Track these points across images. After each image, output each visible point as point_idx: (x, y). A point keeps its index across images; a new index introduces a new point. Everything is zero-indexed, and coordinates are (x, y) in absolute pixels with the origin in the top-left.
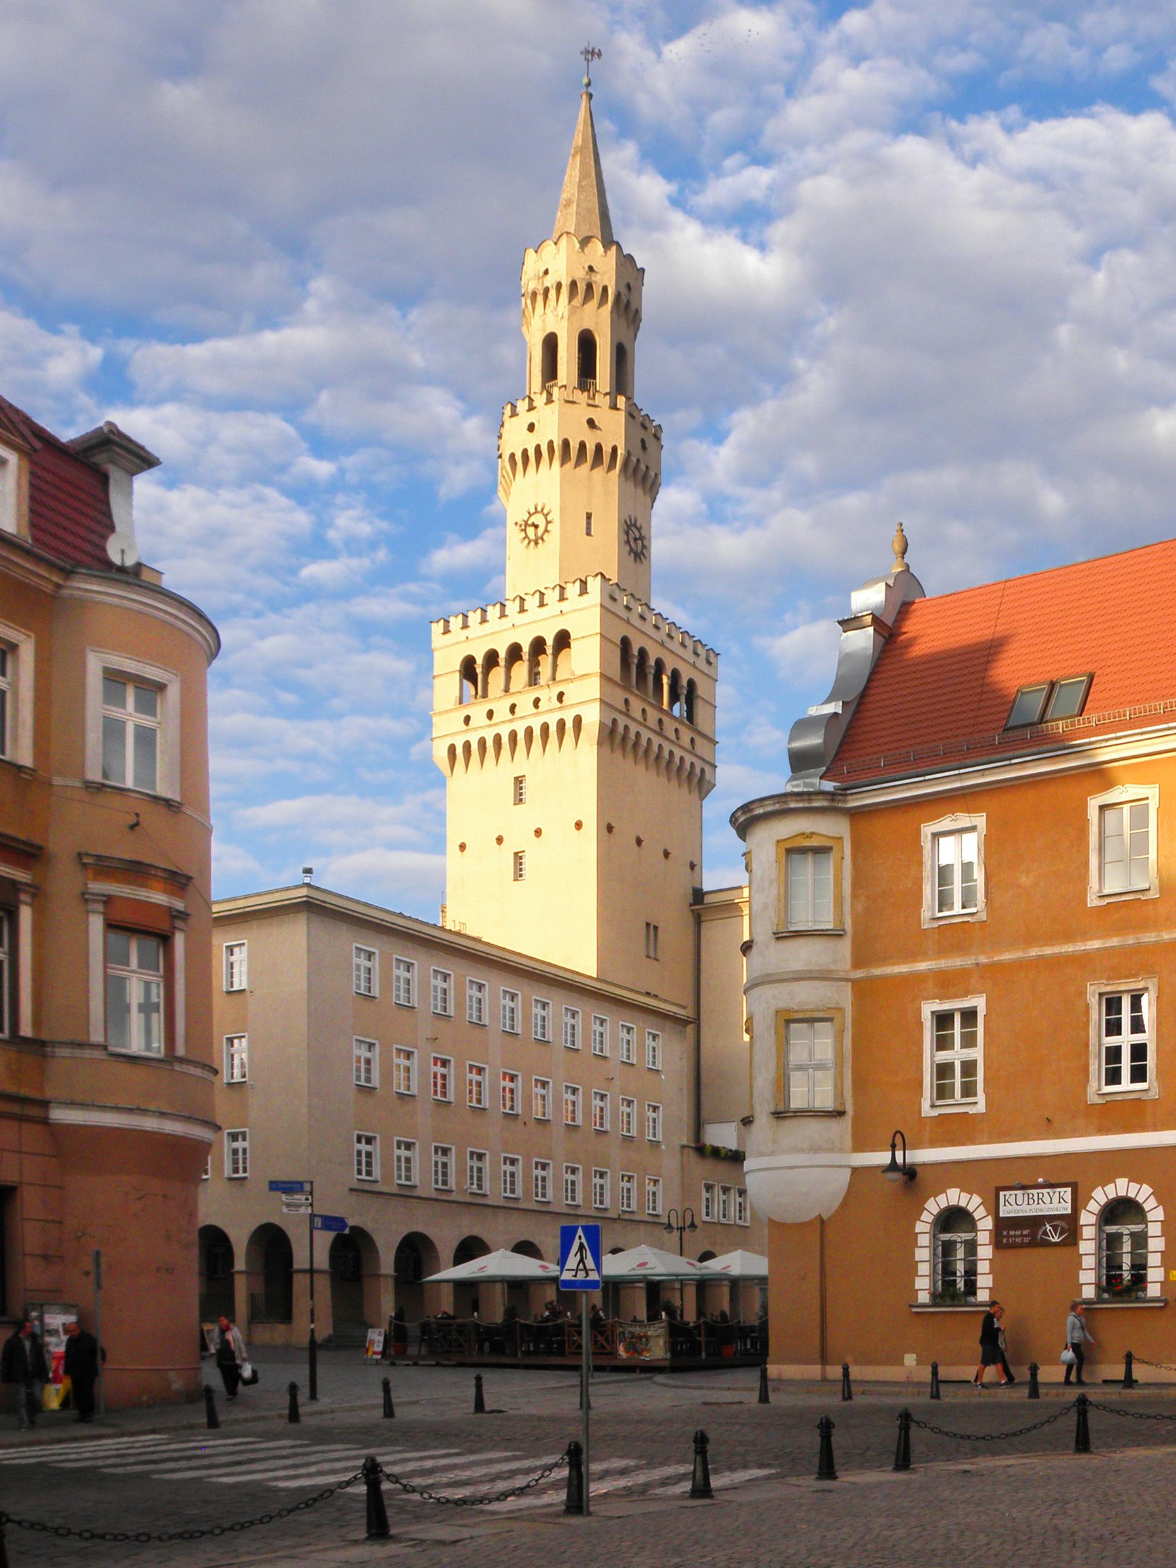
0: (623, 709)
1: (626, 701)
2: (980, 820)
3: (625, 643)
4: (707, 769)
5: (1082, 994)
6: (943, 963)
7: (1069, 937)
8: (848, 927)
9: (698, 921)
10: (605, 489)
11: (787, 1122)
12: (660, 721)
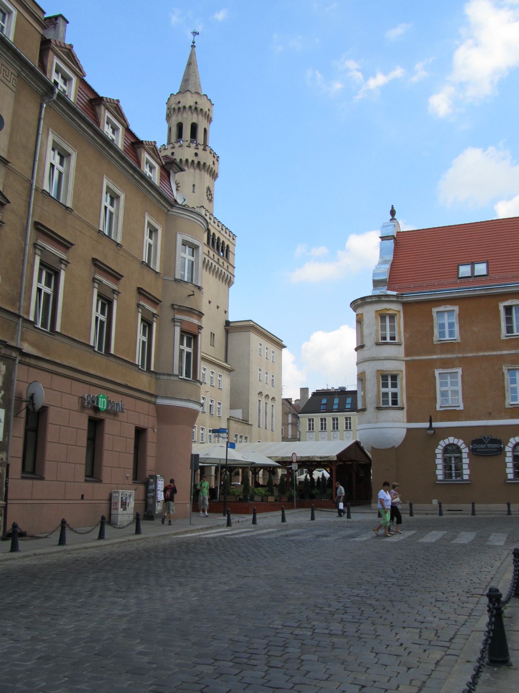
0: (208, 254)
1: (209, 251)
2: (456, 308)
4: (232, 277)
5: (501, 369)
6: (443, 356)
7: (494, 349)
8: (403, 341)
11: (383, 411)
12: (218, 259)
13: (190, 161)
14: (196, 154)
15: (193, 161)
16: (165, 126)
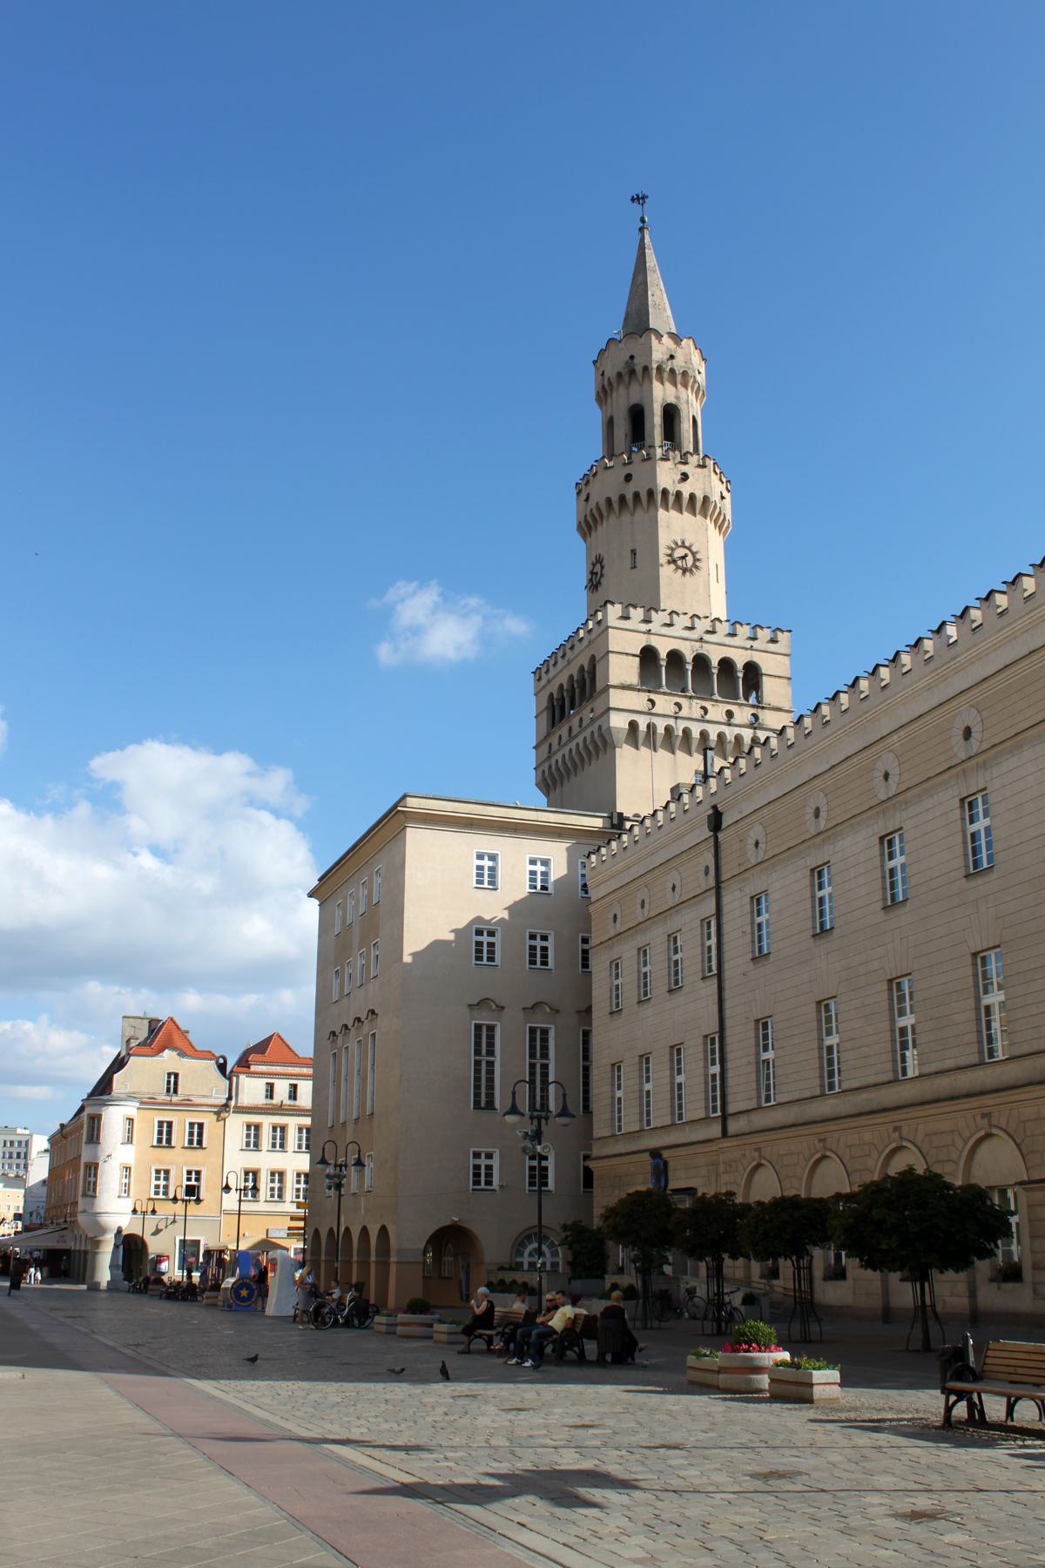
14: (685, 477)
15: (679, 495)
16: (593, 418)
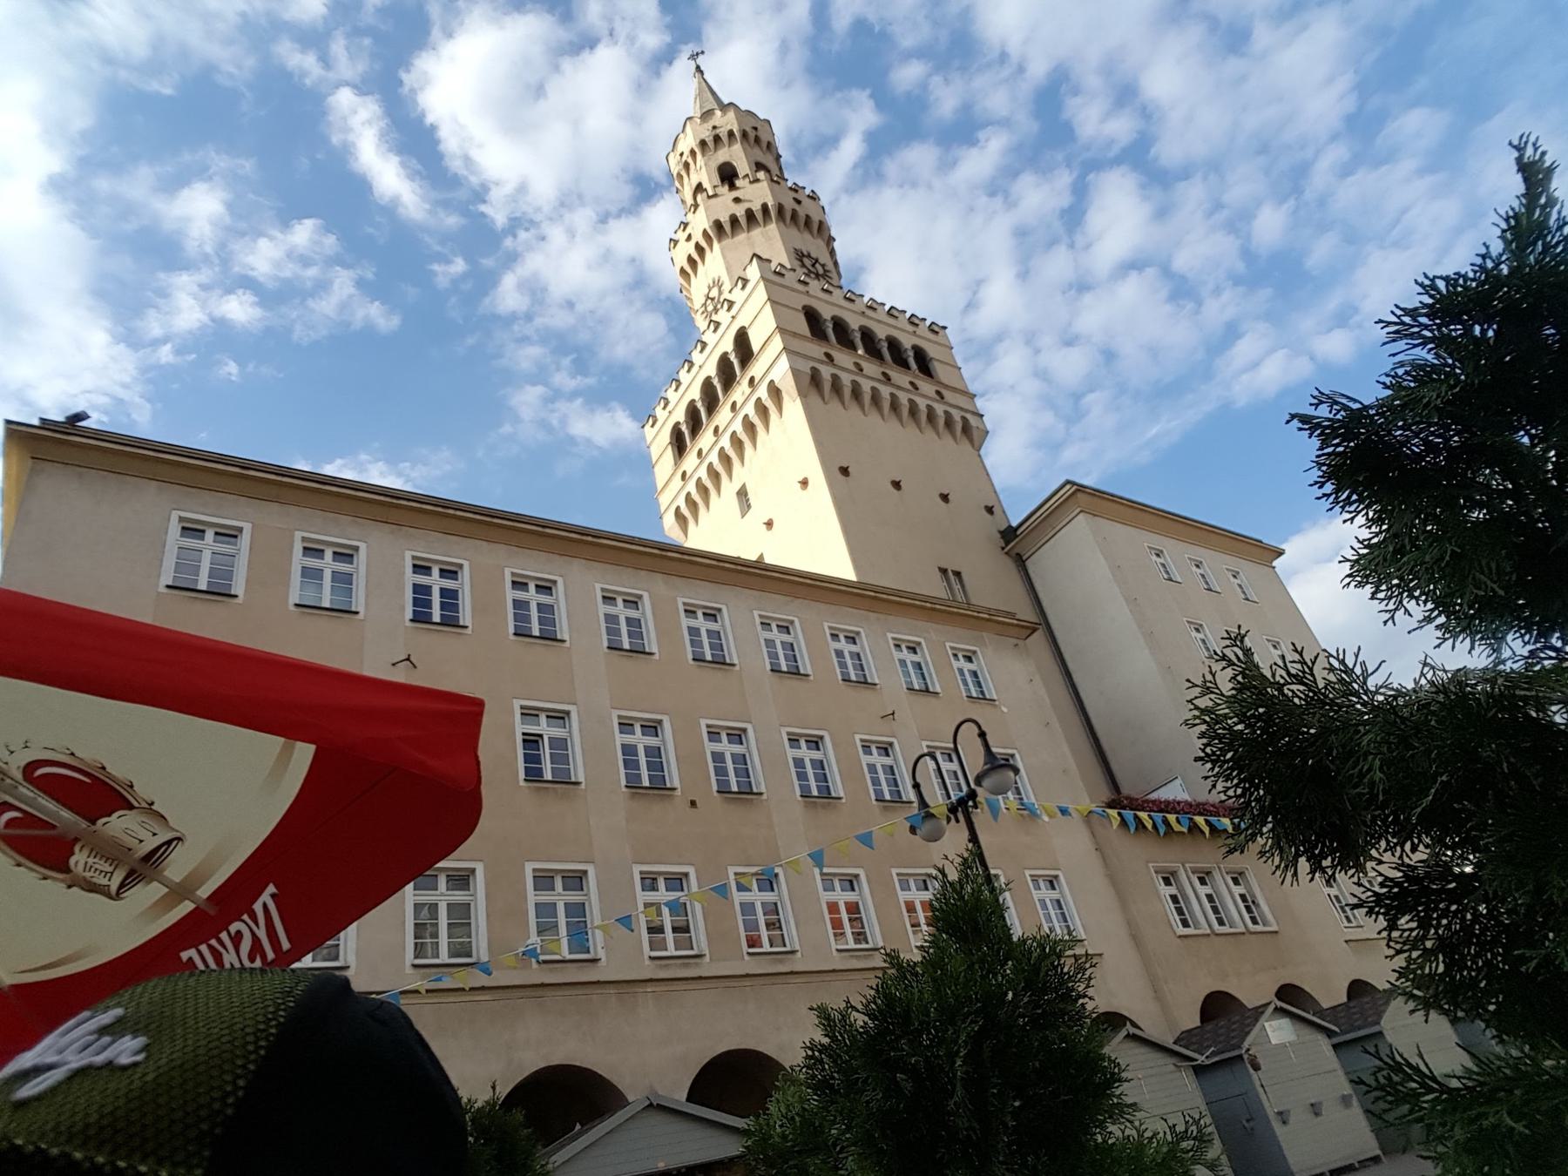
3: (811, 316)
9: (1020, 562)
10: (771, 242)
13: (725, 219)
